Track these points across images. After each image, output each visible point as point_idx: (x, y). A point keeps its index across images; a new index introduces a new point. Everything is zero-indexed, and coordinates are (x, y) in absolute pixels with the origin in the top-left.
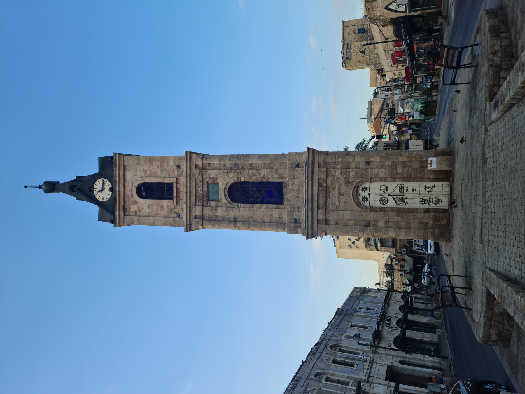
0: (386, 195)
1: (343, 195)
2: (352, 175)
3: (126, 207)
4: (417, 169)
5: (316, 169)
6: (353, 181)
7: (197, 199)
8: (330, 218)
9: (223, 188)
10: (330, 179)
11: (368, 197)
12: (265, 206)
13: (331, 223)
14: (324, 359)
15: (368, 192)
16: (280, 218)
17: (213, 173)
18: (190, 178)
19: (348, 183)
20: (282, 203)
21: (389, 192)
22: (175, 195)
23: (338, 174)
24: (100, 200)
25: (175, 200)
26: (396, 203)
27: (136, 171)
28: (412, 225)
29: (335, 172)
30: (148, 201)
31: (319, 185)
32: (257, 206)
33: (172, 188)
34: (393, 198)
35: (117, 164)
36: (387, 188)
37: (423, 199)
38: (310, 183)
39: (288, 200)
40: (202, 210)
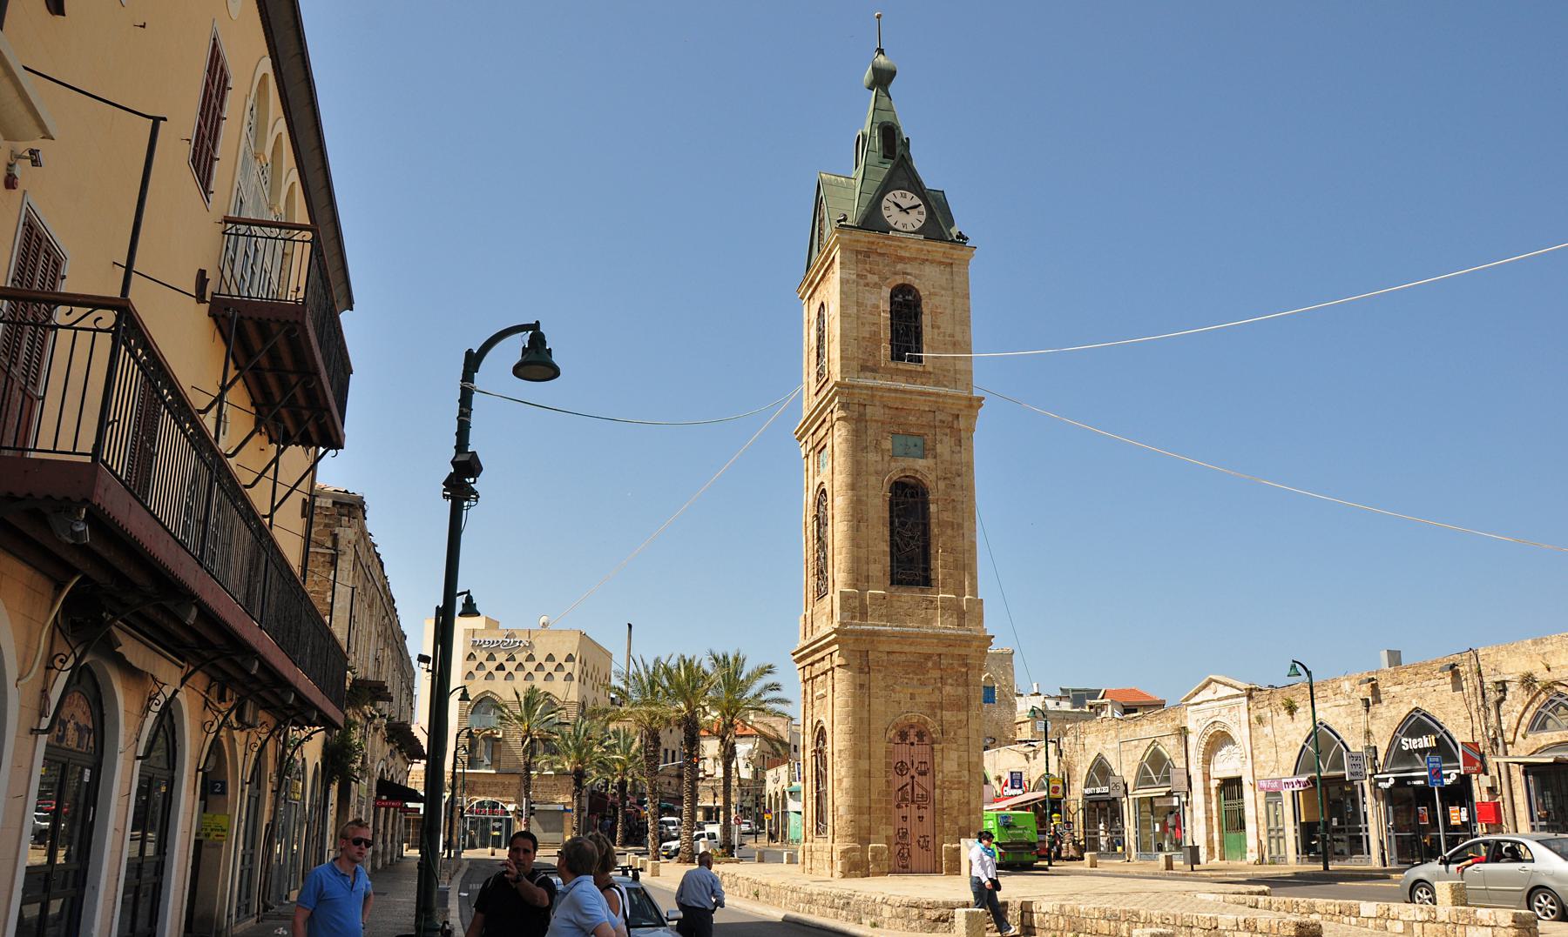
0: (913, 772)
2: (948, 715)
3: (873, 258)
10: (936, 674)
17: (943, 449)
19: (933, 707)
22: (901, 365)
23: (948, 688)
24: (885, 203)
30: (885, 306)
31: (928, 657)
32: (887, 533)
36: (923, 774)
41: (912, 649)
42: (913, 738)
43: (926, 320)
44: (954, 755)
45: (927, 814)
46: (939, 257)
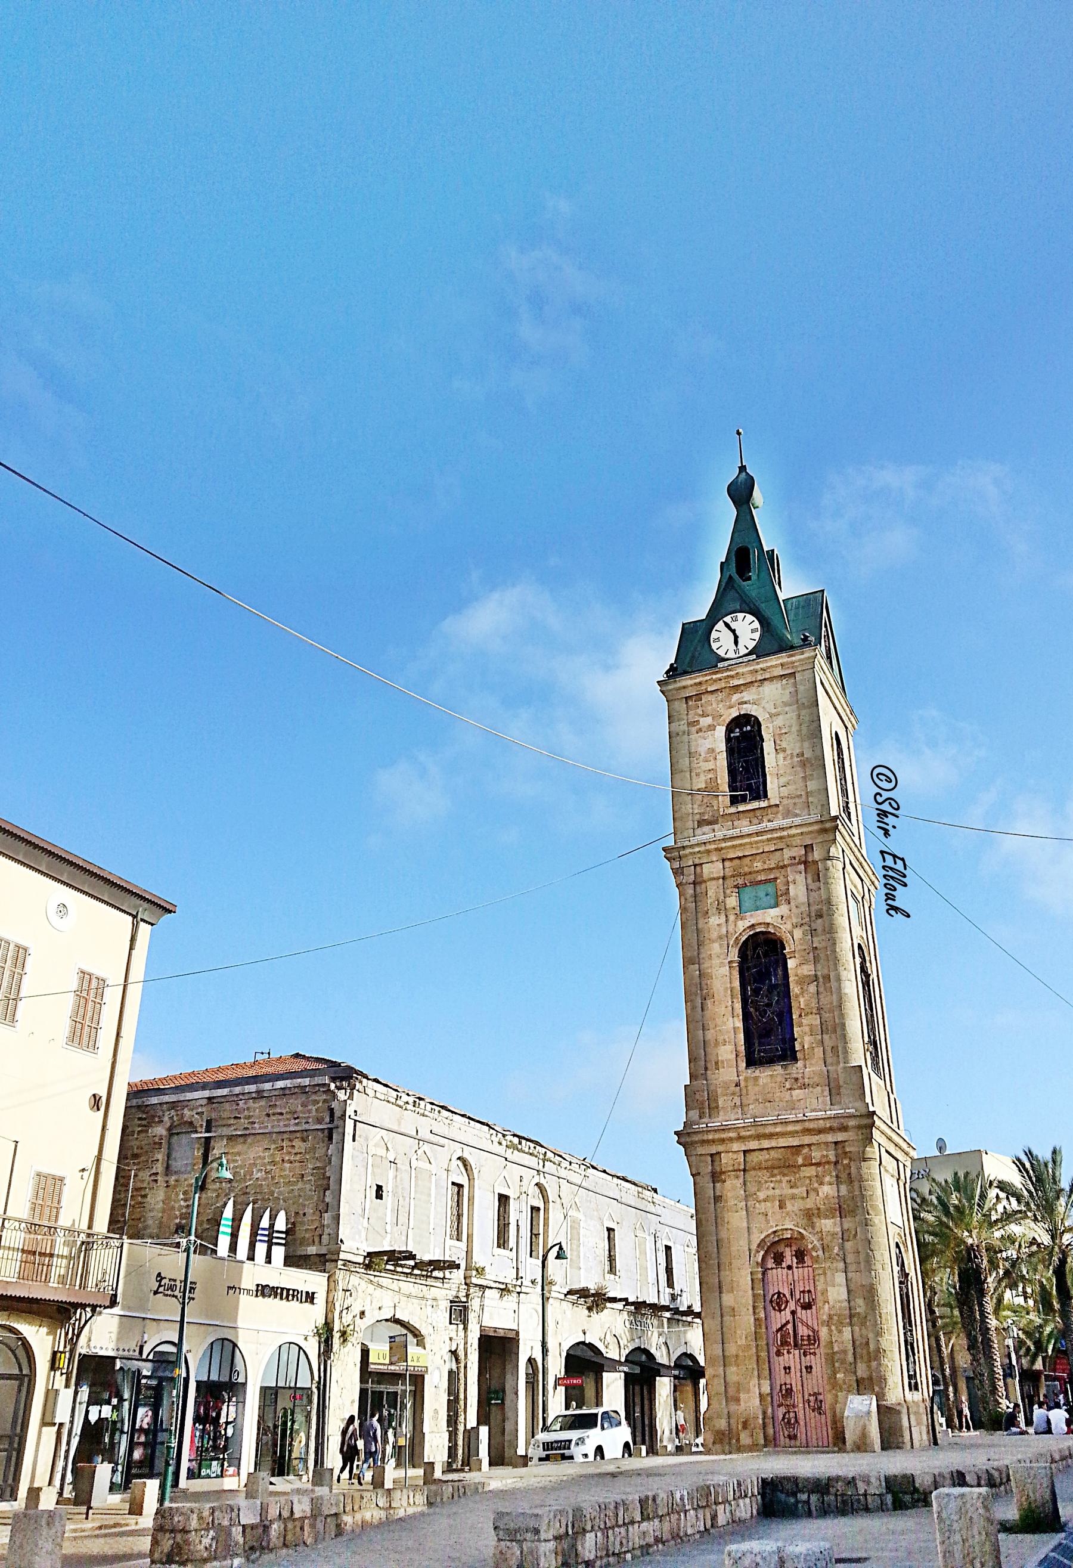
0: (792, 1305)
1: (781, 1207)
4: (855, 1373)
5: (830, 1138)
6: (813, 1228)
7: (737, 862)
8: (728, 1183)
9: (768, 920)
10: (811, 1171)
11: (784, 1265)
12: (740, 1024)
13: (718, 1185)
14: (505, 1173)
15: (795, 1265)
16: (717, 1063)
17: (798, 890)
18: (781, 838)
19: (810, 1215)
20: (752, 1061)
21: (801, 1313)
22: (742, 808)
24: (714, 635)
25: (733, 810)
26: (777, 1331)
27: (785, 704)
28: (734, 1369)
29: (830, 1184)
30: (722, 746)
32: (738, 1006)
33: (757, 798)
34: (788, 1322)
35: (793, 658)
36: (807, 1306)
37: (791, 1389)
38: (798, 1127)
39: (756, 1079)
40: (714, 879)
41: (773, 1143)
42: (789, 1258)
43: (768, 747)
44: (840, 1278)
45: (817, 1362)
46: (780, 672)
